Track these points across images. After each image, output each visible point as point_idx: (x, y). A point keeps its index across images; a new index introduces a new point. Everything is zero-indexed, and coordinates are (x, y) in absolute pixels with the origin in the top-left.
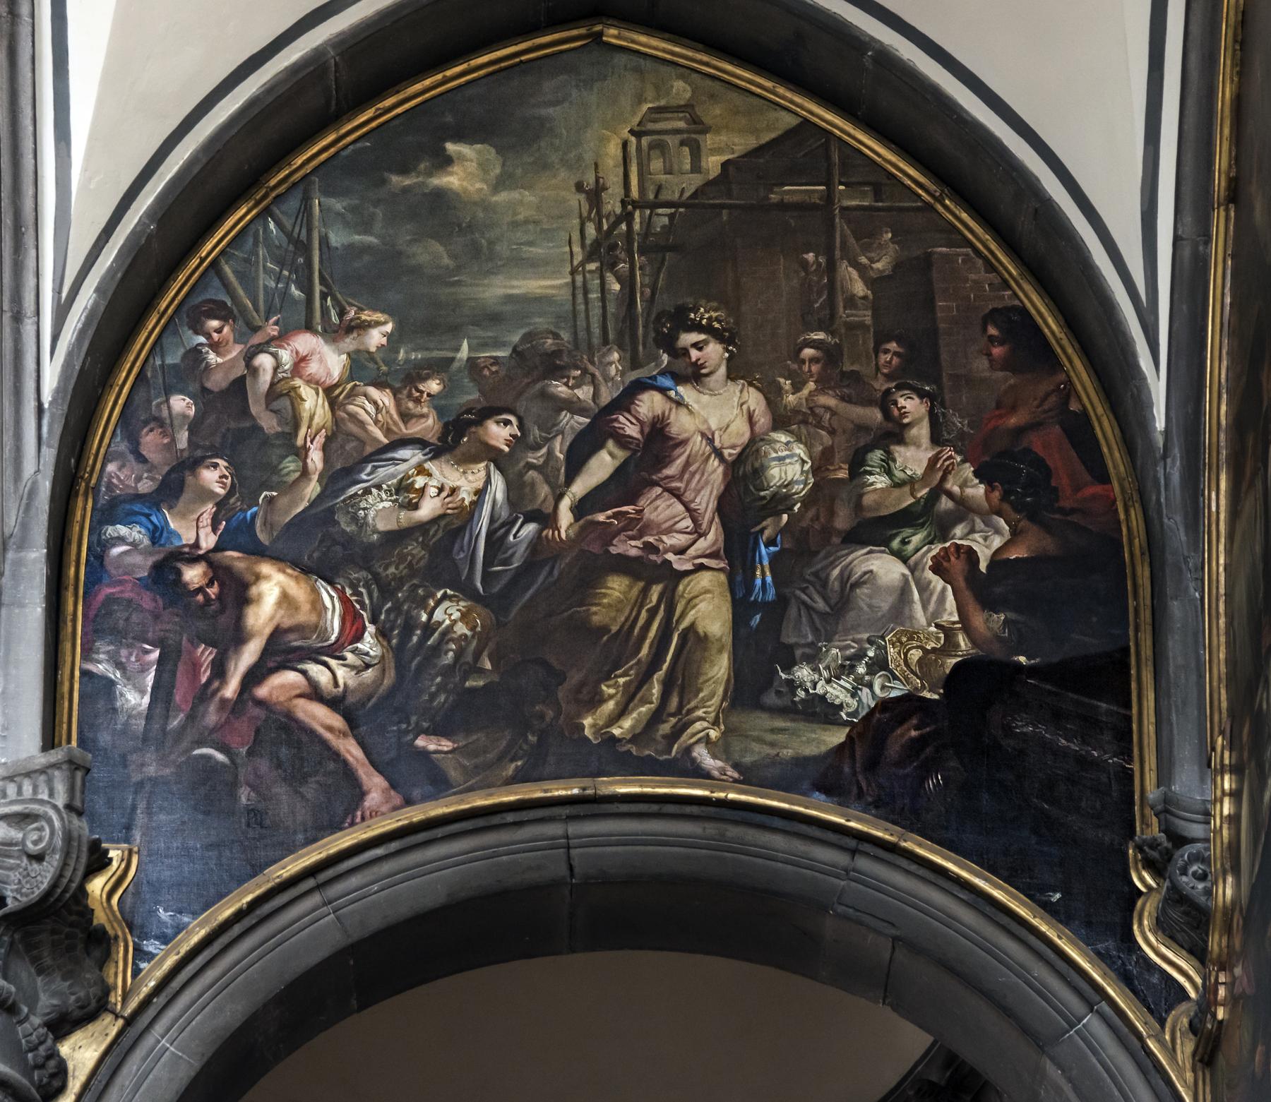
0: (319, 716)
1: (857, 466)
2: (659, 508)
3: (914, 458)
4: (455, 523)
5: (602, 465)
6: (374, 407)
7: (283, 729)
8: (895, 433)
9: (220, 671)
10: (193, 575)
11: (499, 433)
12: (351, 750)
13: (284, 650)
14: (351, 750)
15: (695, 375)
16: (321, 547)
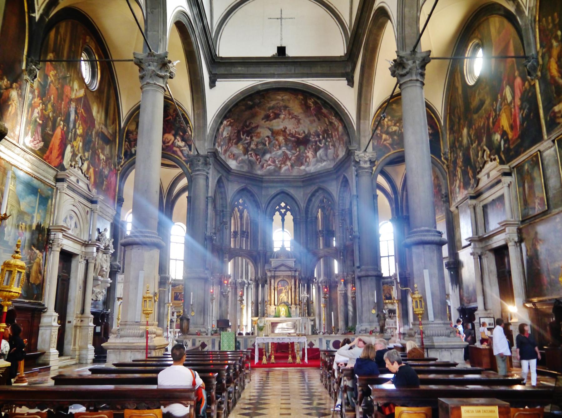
0: (388, 145)
4: (395, 131)
6: (390, 123)
7: (385, 146)
11: (398, 124)
13: (385, 140)
16: (387, 133)
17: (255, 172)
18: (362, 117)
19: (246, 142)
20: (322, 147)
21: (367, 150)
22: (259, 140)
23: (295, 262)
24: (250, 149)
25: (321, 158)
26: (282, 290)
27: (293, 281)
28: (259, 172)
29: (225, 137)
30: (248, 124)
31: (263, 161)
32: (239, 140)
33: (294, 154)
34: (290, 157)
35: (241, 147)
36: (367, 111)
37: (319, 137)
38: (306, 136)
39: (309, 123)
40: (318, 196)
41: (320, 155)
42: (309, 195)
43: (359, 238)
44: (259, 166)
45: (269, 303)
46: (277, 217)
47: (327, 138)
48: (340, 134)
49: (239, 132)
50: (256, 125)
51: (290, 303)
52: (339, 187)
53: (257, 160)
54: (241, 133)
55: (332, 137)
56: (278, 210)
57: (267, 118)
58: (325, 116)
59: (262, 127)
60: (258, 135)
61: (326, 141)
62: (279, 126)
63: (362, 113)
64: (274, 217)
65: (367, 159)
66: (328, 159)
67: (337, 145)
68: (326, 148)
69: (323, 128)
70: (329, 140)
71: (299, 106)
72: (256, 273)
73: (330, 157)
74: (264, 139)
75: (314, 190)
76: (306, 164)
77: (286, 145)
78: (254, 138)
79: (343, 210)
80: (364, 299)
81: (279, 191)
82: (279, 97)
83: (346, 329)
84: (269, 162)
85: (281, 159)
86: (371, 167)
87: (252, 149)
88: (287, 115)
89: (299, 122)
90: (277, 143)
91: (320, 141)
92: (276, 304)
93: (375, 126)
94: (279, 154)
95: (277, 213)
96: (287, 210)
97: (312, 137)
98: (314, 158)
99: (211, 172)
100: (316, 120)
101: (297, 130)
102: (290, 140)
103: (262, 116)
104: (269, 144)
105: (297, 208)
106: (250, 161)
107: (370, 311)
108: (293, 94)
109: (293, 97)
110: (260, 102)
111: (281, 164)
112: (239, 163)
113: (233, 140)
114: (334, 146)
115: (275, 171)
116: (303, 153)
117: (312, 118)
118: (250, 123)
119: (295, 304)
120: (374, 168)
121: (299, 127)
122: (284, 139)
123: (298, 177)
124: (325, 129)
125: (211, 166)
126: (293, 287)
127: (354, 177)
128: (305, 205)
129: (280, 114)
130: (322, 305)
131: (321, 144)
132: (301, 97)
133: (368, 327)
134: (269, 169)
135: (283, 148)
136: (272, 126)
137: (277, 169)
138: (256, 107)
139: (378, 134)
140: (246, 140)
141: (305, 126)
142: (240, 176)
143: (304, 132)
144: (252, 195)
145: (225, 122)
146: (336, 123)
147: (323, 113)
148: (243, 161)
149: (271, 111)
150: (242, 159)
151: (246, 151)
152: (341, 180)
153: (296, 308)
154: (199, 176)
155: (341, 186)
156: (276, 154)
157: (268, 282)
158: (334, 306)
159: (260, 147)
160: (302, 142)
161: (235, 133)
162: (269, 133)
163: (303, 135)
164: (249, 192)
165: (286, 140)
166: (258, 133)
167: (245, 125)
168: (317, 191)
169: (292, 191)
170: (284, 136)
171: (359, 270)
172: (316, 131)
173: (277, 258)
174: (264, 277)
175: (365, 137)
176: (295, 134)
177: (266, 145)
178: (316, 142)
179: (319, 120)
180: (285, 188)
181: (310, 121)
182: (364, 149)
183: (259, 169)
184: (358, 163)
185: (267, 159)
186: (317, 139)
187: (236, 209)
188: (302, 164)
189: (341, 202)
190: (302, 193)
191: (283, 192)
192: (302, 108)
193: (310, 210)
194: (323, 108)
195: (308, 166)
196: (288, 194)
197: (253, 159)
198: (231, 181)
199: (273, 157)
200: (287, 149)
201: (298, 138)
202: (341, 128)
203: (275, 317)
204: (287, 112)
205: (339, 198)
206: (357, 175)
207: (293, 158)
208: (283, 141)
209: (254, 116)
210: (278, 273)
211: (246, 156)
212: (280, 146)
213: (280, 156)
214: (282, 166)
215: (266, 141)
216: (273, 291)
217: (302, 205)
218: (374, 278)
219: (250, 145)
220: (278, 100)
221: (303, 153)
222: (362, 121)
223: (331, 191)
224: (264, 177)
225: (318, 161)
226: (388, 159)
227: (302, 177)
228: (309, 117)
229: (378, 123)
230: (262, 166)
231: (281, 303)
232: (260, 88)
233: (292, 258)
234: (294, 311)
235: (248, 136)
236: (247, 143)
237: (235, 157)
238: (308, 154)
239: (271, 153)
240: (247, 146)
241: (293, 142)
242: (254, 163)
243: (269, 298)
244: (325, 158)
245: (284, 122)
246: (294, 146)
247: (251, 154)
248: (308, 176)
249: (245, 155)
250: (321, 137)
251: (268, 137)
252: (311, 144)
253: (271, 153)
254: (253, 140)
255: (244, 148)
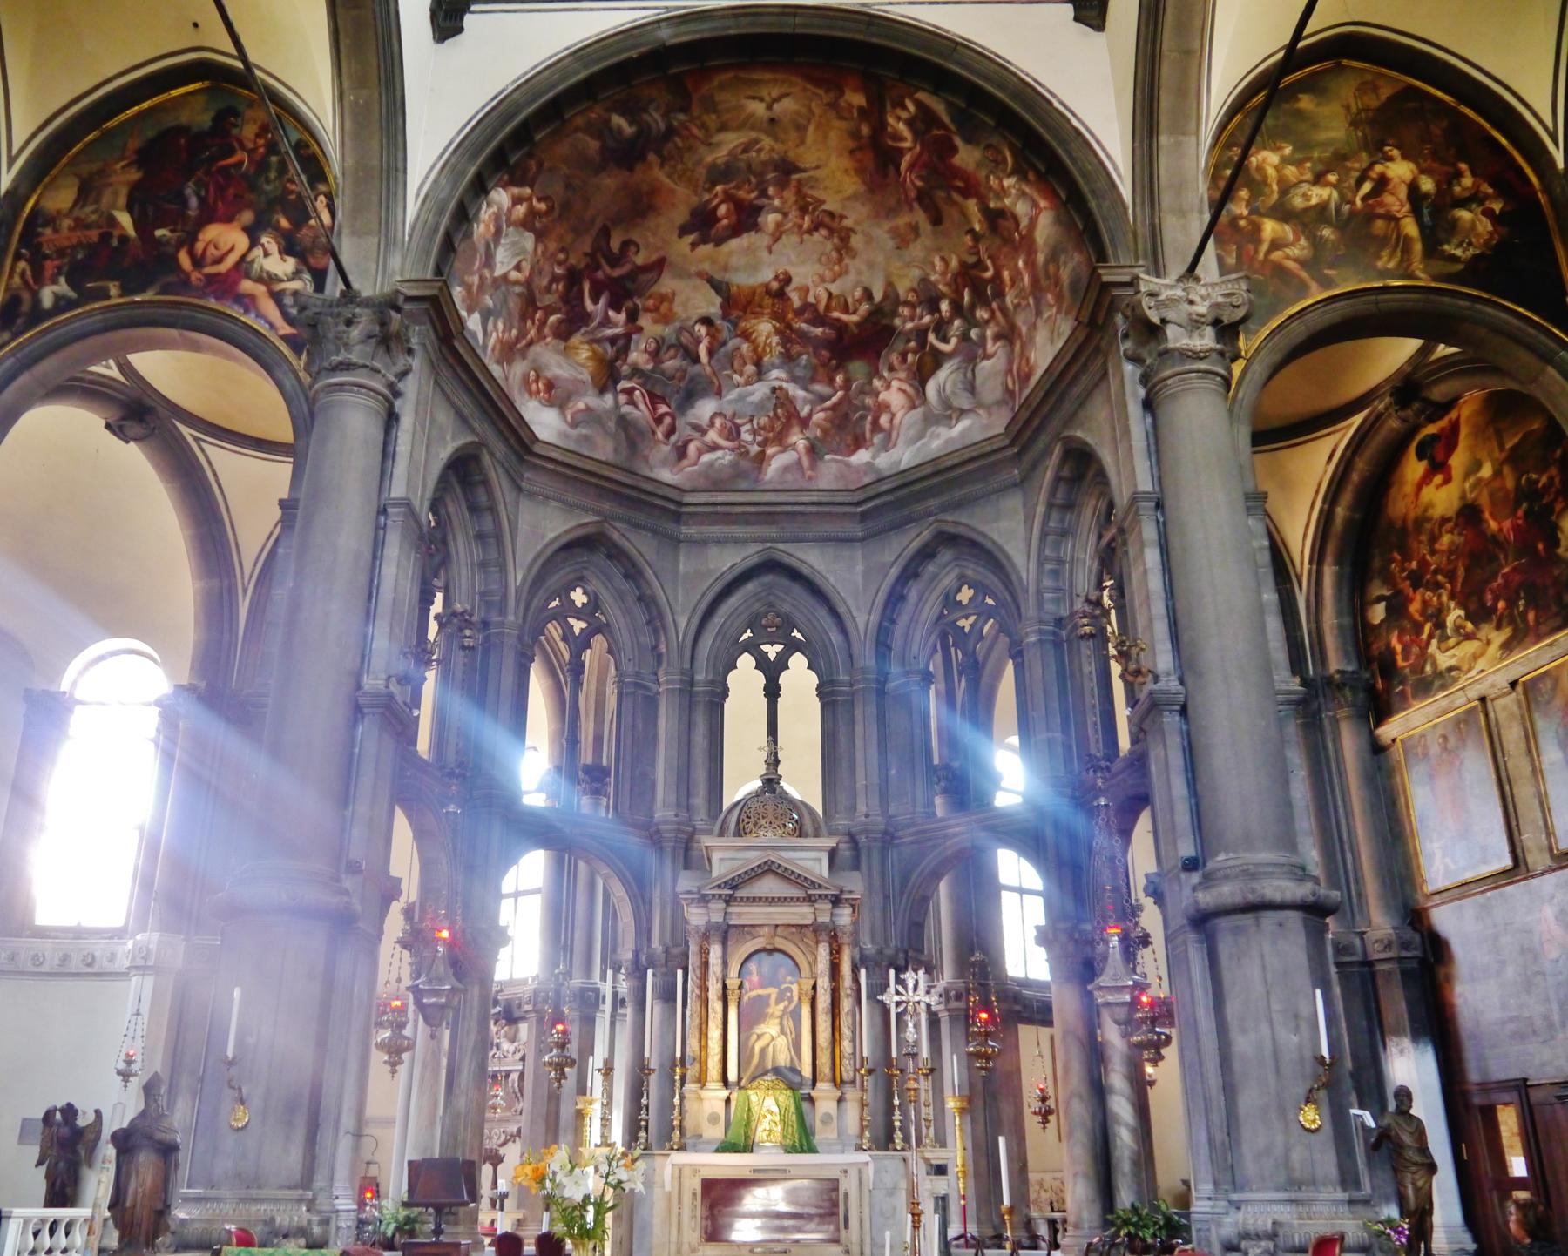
0: (1291, 265)
1: (1450, 185)
2: (1388, 198)
3: (1468, 181)
4: (1322, 208)
5: (1367, 187)
6: (1291, 172)
7: (1280, 270)
8: (1459, 175)
9: (1256, 251)
10: (1242, 223)
11: (1332, 178)
12: (1304, 274)
13: (1276, 245)
14: (1304, 274)
15: (1391, 159)
16: (1283, 213)
17: (646, 472)
18: (1164, 120)
19: (609, 332)
20: (950, 355)
21: (1199, 271)
22: (667, 331)
23: (833, 854)
24: (625, 369)
25: (946, 404)
26: (762, 1001)
27: (823, 951)
28: (666, 475)
29: (505, 277)
30: (615, 244)
31: (683, 431)
32: (574, 321)
33: (824, 399)
34: (804, 412)
35: (584, 353)
36: (1189, 90)
37: (934, 308)
38: (877, 312)
39: (891, 244)
40: (935, 576)
41: (941, 390)
42: (894, 572)
43: (1184, 711)
44: (666, 449)
45: (692, 1071)
46: (745, 678)
47: (972, 308)
48: (1041, 258)
49: (573, 278)
50: (654, 258)
51: (807, 1072)
52: (1041, 509)
53: (659, 420)
54: (587, 287)
55: (999, 294)
56: (752, 647)
57: (702, 225)
58: (971, 188)
59: (683, 274)
60: (664, 308)
61: (971, 322)
62: (755, 268)
63: (1166, 101)
64: (732, 679)
65: (1202, 308)
66: (980, 405)
67: (1022, 322)
68: (971, 353)
69: (954, 263)
70: (982, 314)
71: (846, 162)
72: (643, 930)
73: (991, 389)
74: (691, 332)
75: (916, 544)
76: (877, 439)
77: (788, 358)
78: (645, 321)
79: (1059, 622)
80: (1242, 1044)
81: (755, 560)
82: (758, 108)
83: (1106, 1224)
84: (712, 435)
85: (764, 421)
86: (1221, 354)
87: (636, 371)
88: (794, 214)
89: (844, 247)
90: (745, 347)
91: (941, 328)
92: (732, 1075)
93: (1222, 184)
94: (756, 398)
95: (746, 661)
96: (792, 647)
97: (905, 311)
98: (913, 407)
99: (410, 386)
100: (925, 226)
101: (835, 288)
102: (803, 337)
103: (680, 215)
104: (711, 353)
105: (835, 638)
106: (623, 422)
107: (1284, 1112)
108: (818, 82)
109: (819, 99)
110: (671, 131)
111: (764, 444)
112: (574, 425)
113: (549, 311)
114: (1008, 335)
115: (737, 472)
116: (862, 392)
117: (903, 220)
118: (626, 244)
119: (837, 1082)
120: (1237, 368)
121: (844, 272)
122: (778, 332)
123: (840, 498)
124: (963, 264)
125: (416, 362)
126: (824, 983)
127: (1134, 409)
128: (875, 618)
129: (758, 210)
130: (951, 1104)
131: (945, 340)
132: (857, 99)
133: (1284, 1214)
134: (711, 464)
135: (775, 373)
136: (725, 268)
137: (745, 464)
138: (652, 157)
139: (1241, 217)
140: (606, 322)
141: (871, 265)
142: (573, 474)
143: (868, 294)
144: (633, 573)
145: (501, 197)
146: (1022, 209)
147: (957, 173)
148: (590, 416)
149: (719, 188)
150: (588, 409)
151: (607, 376)
152: (1049, 475)
153: (840, 1100)
154: (337, 397)
155: (1050, 506)
156: (741, 398)
157: (694, 960)
158: (1007, 1110)
159: (671, 364)
160: (858, 341)
161: (555, 279)
162: (710, 304)
163: (865, 308)
164: (617, 554)
165: (788, 335)
166: (663, 298)
167: (600, 252)
168: (926, 554)
169: (812, 559)
170: (778, 316)
171: (1195, 878)
172: (924, 280)
173: (739, 832)
174: (675, 951)
175: (1182, 213)
176: (828, 308)
177: (697, 360)
178: (921, 334)
179: (937, 220)
180: (781, 546)
181: (894, 233)
182: (1184, 268)
183: (664, 463)
184: (1152, 331)
185: (704, 421)
186: (927, 319)
187: (554, 629)
188: (859, 443)
189: (1048, 582)
190: (860, 568)
191: (770, 566)
192: (860, 171)
193: (897, 644)
194: (958, 141)
195: (887, 445)
196: (795, 575)
197: (641, 412)
198: (532, 495)
199: (729, 413)
200: (794, 379)
201: (840, 327)
202: (1045, 229)
203: (727, 1147)
204: (789, 194)
205: (1040, 564)
206: (1149, 405)
207: (819, 417)
208: (775, 340)
209: (641, 206)
210: (743, 914)
211: (608, 399)
212: (758, 363)
213: (760, 406)
214: (770, 451)
215: (699, 342)
216: (716, 1006)
217: (861, 620)
218: (1294, 919)
219: (625, 350)
220: (748, 123)
221: (862, 392)
222: (1164, 140)
223: (995, 537)
224: (688, 499)
225: (930, 420)
226: (1299, 331)
227: (856, 498)
228: (891, 212)
229: (1232, 177)
230: (681, 452)
231: (757, 1071)
232: (666, 35)
233: (817, 835)
234: (827, 1119)
235: (615, 305)
236: (613, 340)
237: (554, 394)
238: (881, 397)
239: (719, 394)
240: (610, 351)
241: (817, 344)
242: (641, 433)
243: (693, 1043)
244: (963, 401)
245: (775, 247)
246: (824, 365)
247: (629, 392)
248: (884, 488)
249: (602, 391)
250: (944, 306)
251: (707, 321)
252: (899, 345)
253: (719, 394)
254: (640, 330)
255: (598, 358)
